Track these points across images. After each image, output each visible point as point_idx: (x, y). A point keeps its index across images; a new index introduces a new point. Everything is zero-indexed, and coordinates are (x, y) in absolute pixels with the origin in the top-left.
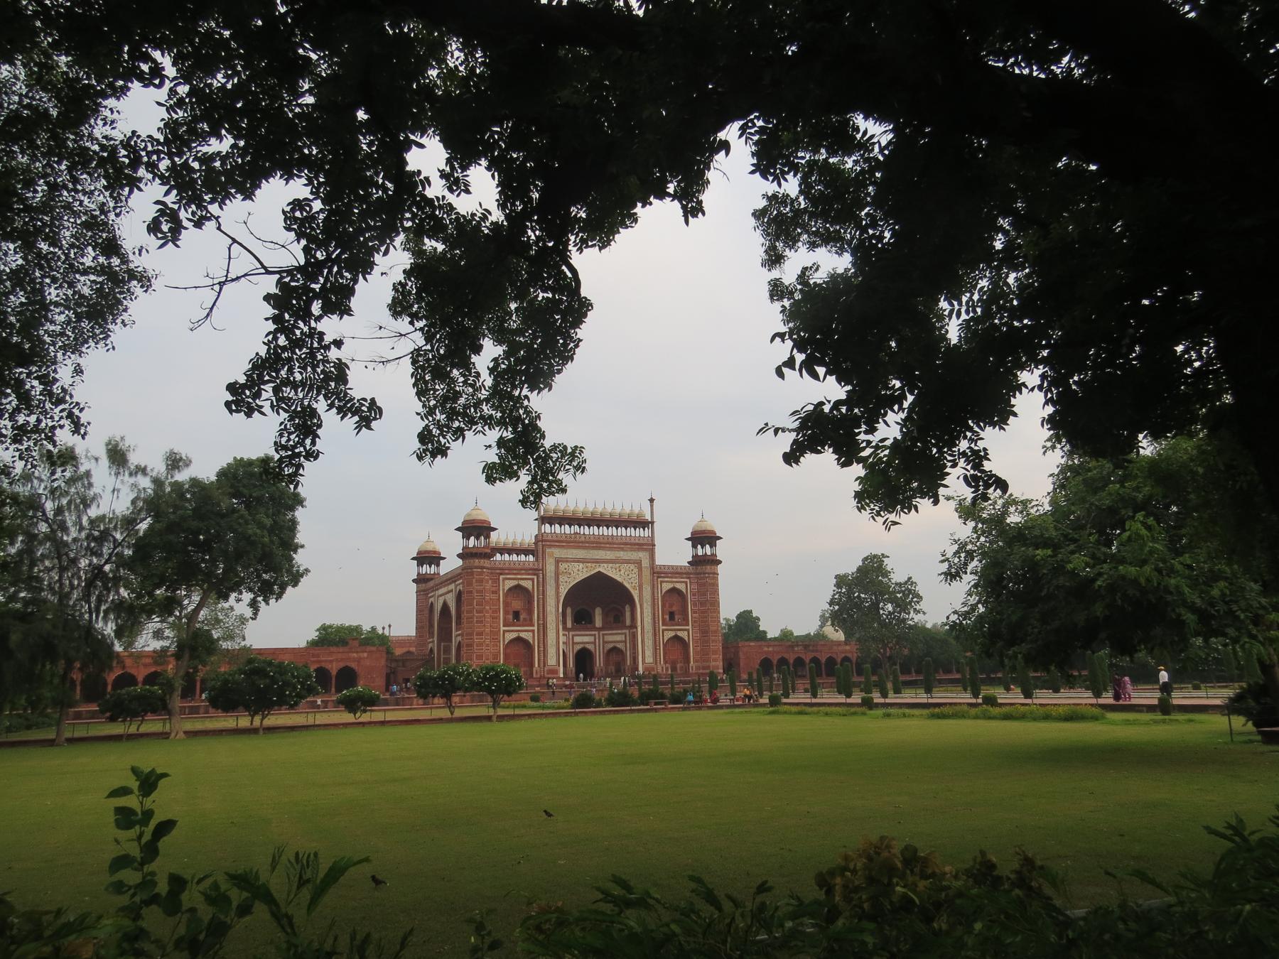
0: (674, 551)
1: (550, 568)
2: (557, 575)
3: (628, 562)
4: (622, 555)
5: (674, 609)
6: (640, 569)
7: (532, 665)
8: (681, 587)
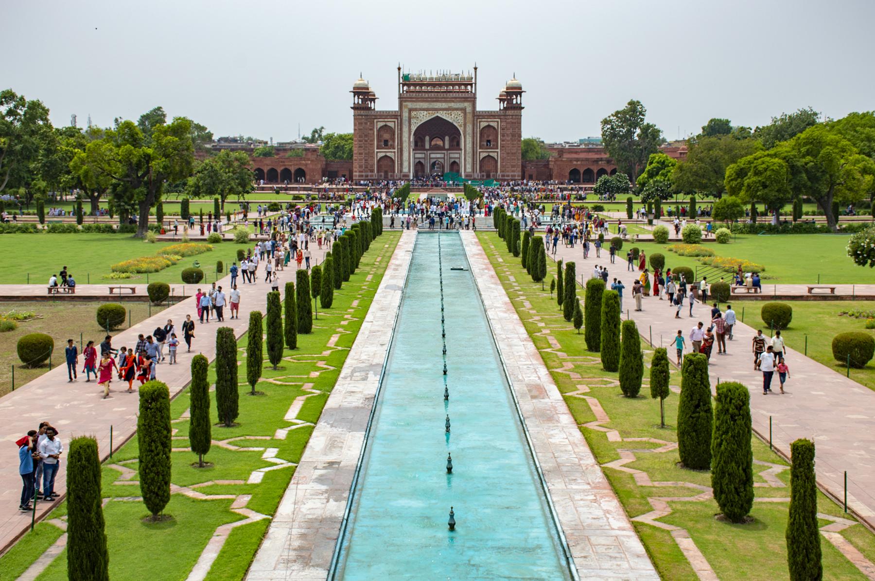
0: (488, 101)
1: (405, 115)
2: (410, 118)
3: (457, 109)
4: (452, 105)
5: (490, 138)
6: (465, 114)
7: (394, 172)
8: (494, 124)
